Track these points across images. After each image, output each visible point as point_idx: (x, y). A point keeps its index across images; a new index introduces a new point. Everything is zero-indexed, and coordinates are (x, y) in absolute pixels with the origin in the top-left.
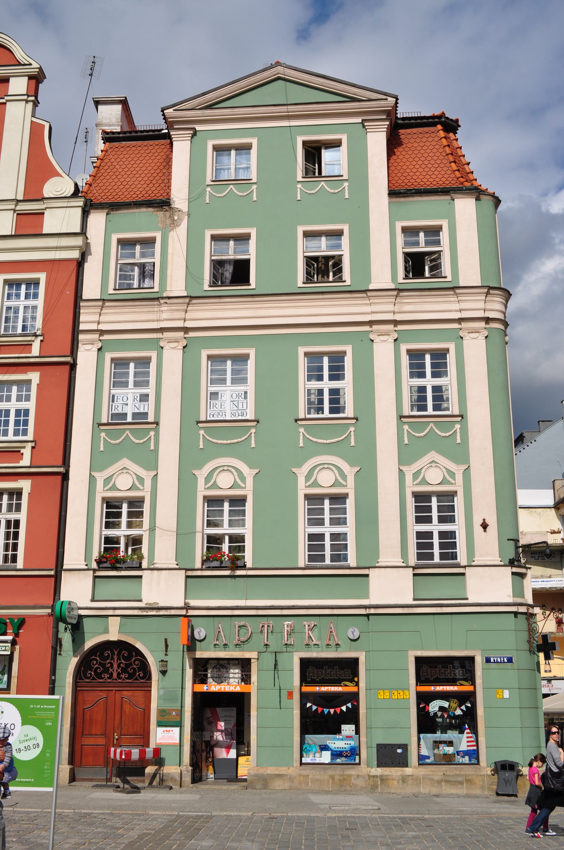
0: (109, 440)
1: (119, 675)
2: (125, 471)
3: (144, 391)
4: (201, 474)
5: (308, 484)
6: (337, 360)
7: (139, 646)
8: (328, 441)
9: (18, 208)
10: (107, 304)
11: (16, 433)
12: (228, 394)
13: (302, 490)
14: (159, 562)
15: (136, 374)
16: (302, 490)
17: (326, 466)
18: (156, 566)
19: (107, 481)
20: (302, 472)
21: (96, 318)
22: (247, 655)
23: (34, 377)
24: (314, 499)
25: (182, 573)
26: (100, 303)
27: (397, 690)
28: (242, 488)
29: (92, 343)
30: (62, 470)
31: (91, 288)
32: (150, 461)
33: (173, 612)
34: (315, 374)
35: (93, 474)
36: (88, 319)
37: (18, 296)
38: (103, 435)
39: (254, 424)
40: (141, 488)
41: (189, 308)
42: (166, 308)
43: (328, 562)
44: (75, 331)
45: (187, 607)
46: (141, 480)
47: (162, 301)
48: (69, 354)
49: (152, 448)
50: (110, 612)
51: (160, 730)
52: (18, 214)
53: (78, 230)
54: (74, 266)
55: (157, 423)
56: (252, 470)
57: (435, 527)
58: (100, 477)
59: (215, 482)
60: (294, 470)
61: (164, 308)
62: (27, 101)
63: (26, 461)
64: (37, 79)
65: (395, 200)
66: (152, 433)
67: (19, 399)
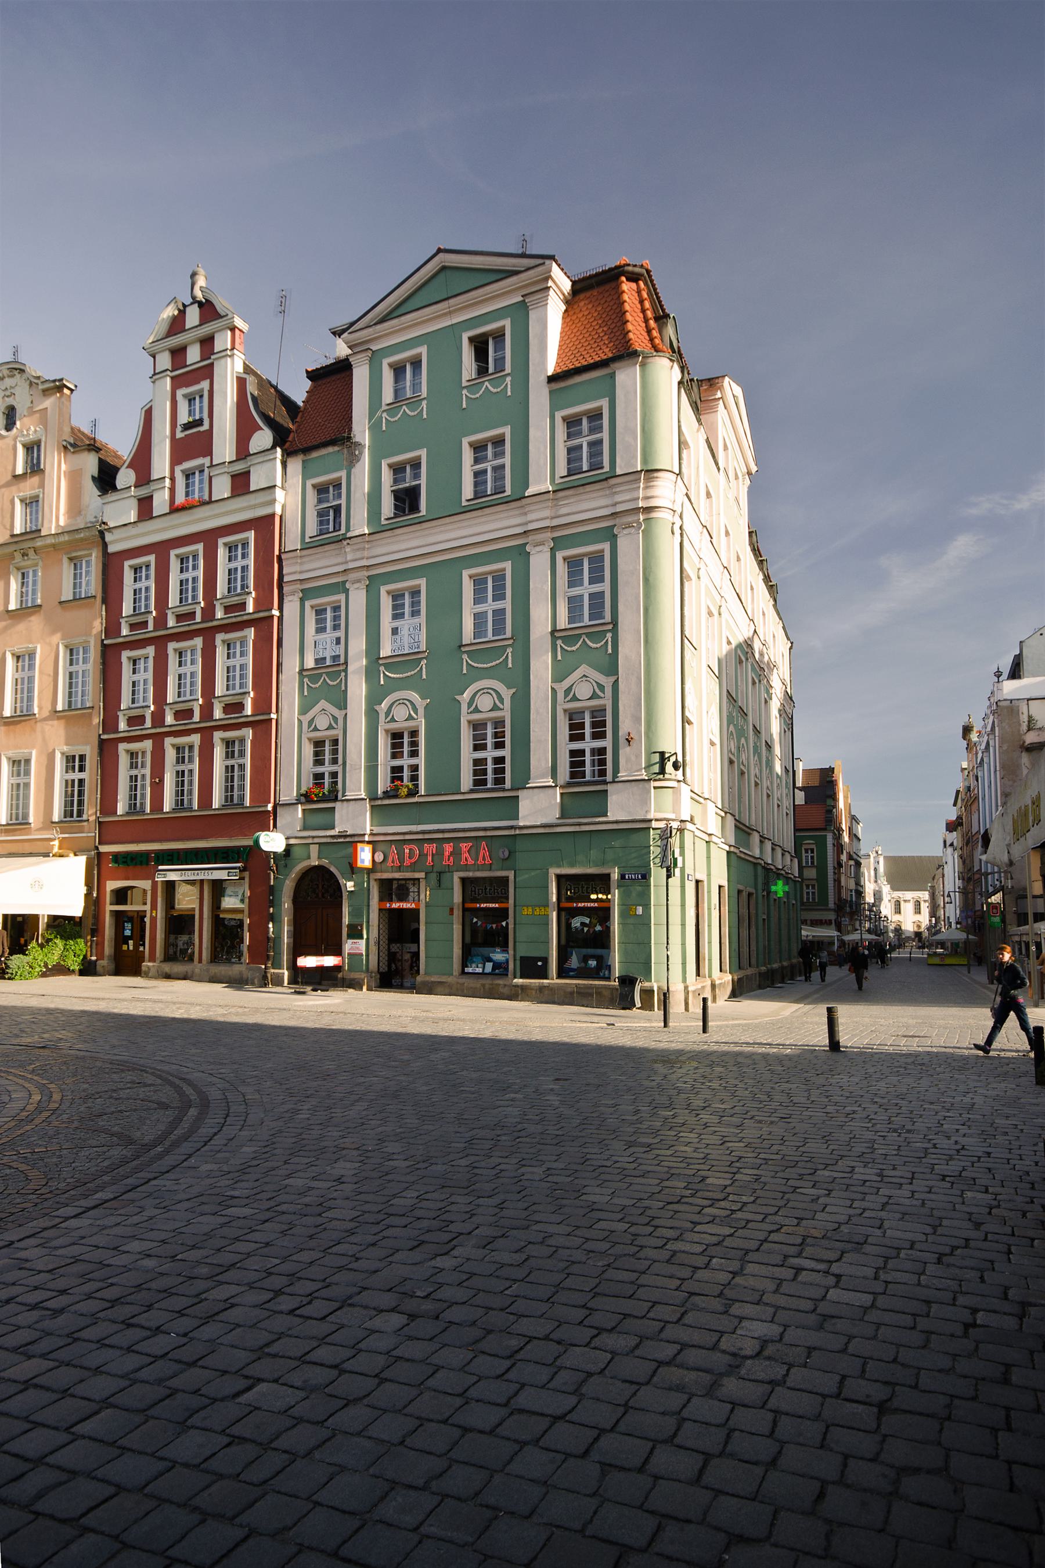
1: (323, 894)
3: (337, 634)
6: (499, 578)
7: (332, 869)
12: (406, 627)
14: (350, 795)
22: (417, 875)
24: (477, 726)
27: (539, 906)
29: (293, 593)
43: (489, 786)
47: (345, 543)
51: (350, 941)
57: (588, 745)
61: (348, 549)
65: (556, 386)
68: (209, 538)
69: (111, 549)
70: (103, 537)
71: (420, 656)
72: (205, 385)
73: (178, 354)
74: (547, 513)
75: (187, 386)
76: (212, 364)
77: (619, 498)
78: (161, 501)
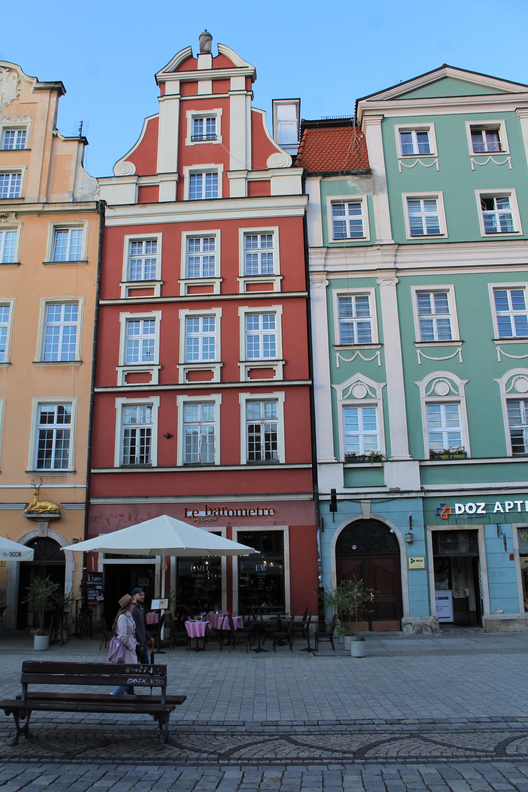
0: (343, 359)
2: (359, 383)
4: (422, 385)
5: (508, 390)
8: (520, 357)
9: (249, 177)
10: (331, 251)
11: (266, 354)
13: (504, 396)
15: (357, 306)
16: (504, 396)
17: (521, 376)
18: (394, 458)
19: (345, 392)
20: (502, 382)
21: (322, 262)
23: (278, 309)
25: (417, 464)
26: (325, 250)
28: (456, 395)
31: (315, 237)
32: (378, 374)
33: (414, 495)
34: (501, 304)
35: (333, 386)
36: (316, 262)
37: (256, 245)
38: (338, 354)
39: (460, 344)
40: (374, 396)
41: (398, 254)
42: (380, 254)
44: (307, 273)
45: (422, 490)
46: (373, 390)
48: (305, 290)
49: (379, 364)
50: (363, 497)
52: (248, 182)
53: (301, 193)
55: (382, 345)
56: (379, 384)
58: (339, 389)
59: (434, 390)
60: (495, 380)
61: (379, 253)
62: (246, 95)
64: (251, 79)
66: (378, 353)
67: (265, 327)
69: (108, 223)
71: (456, 344)
74: (380, 259)
77: (369, 260)
78: (167, 191)
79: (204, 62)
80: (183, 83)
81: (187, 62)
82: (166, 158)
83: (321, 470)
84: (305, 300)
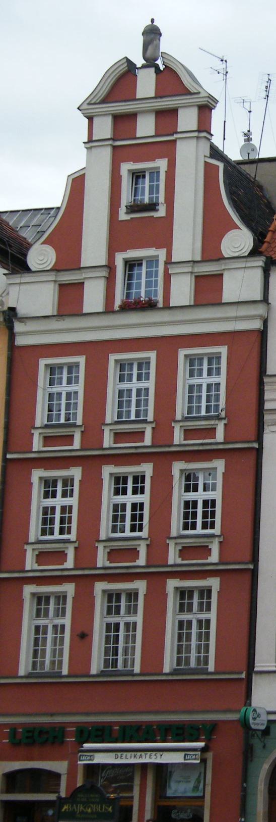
30: (251, 567)
53: (258, 296)
54: (256, 339)
63: (214, 557)
68: (167, 346)
70: (11, 328)
72: (162, 164)
73: (124, 122)
75: (135, 161)
76: (175, 141)
78: (93, 296)
79: (146, 84)
80: (117, 118)
81: (123, 80)
82: (94, 246)
83: (256, 680)
84: (254, 453)
